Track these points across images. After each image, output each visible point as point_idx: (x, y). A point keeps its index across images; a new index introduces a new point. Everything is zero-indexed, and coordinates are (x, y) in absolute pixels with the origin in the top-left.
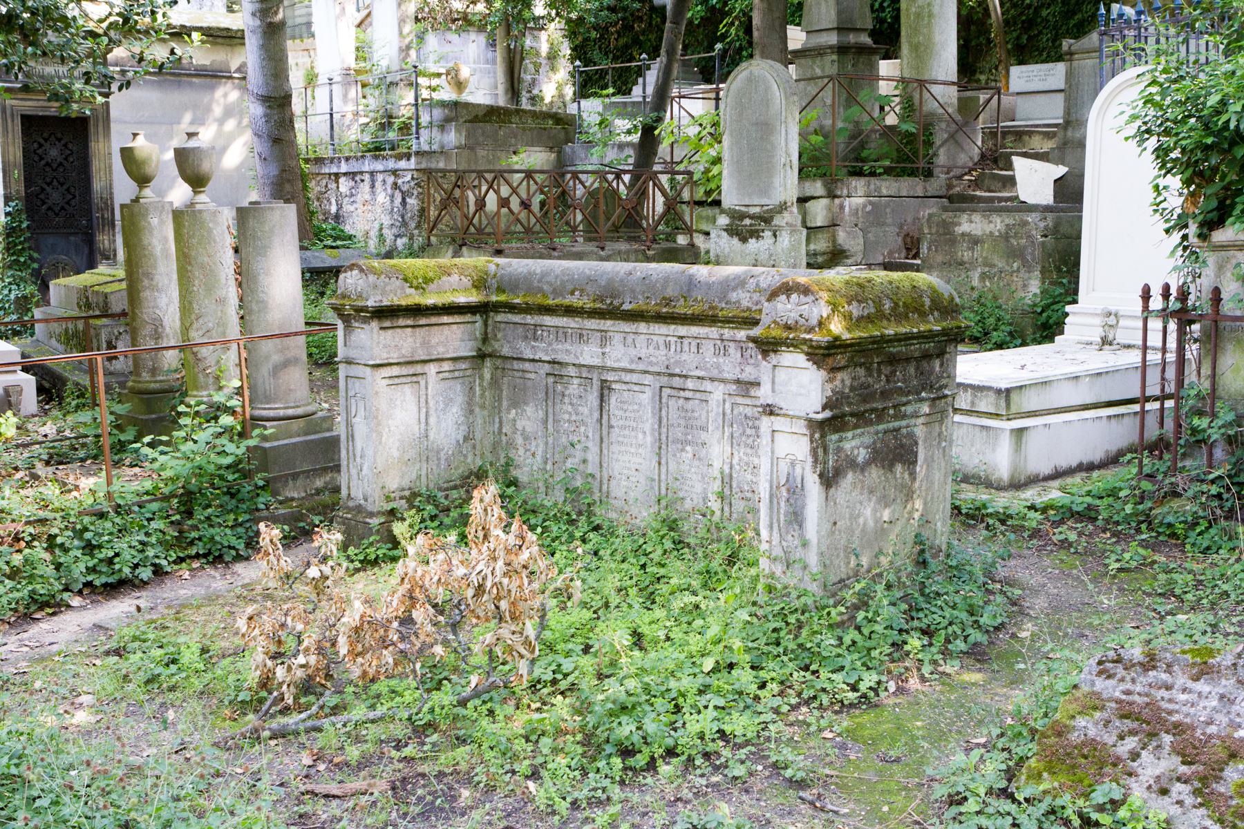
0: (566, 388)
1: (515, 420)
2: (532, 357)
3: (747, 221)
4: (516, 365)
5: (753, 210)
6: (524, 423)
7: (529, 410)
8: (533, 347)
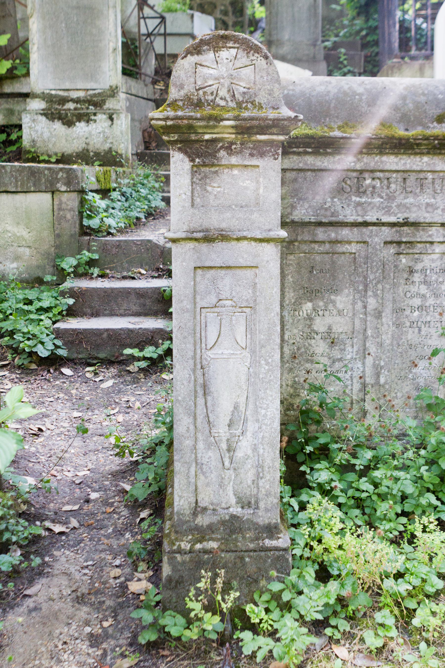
0: (417, 261)
1: (310, 318)
2: (360, 220)
3: (71, 106)
4: (321, 234)
5: (74, 95)
6: (328, 320)
7: (342, 300)
8: (359, 204)
